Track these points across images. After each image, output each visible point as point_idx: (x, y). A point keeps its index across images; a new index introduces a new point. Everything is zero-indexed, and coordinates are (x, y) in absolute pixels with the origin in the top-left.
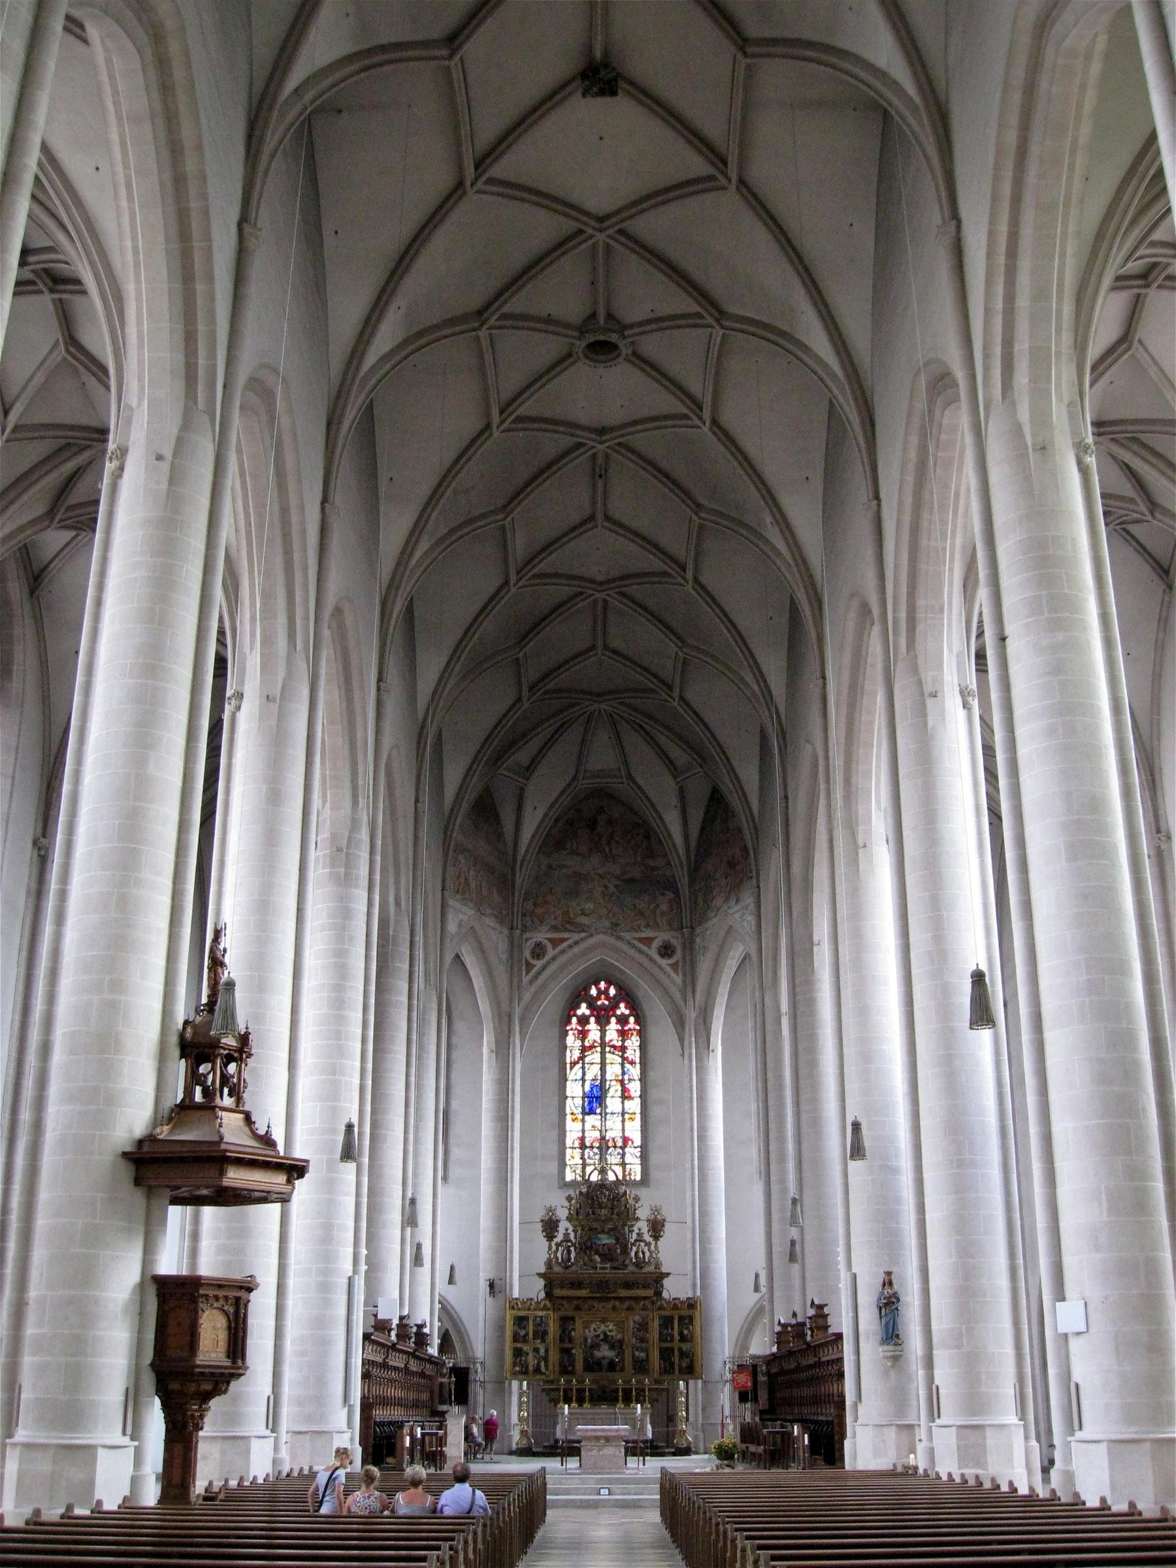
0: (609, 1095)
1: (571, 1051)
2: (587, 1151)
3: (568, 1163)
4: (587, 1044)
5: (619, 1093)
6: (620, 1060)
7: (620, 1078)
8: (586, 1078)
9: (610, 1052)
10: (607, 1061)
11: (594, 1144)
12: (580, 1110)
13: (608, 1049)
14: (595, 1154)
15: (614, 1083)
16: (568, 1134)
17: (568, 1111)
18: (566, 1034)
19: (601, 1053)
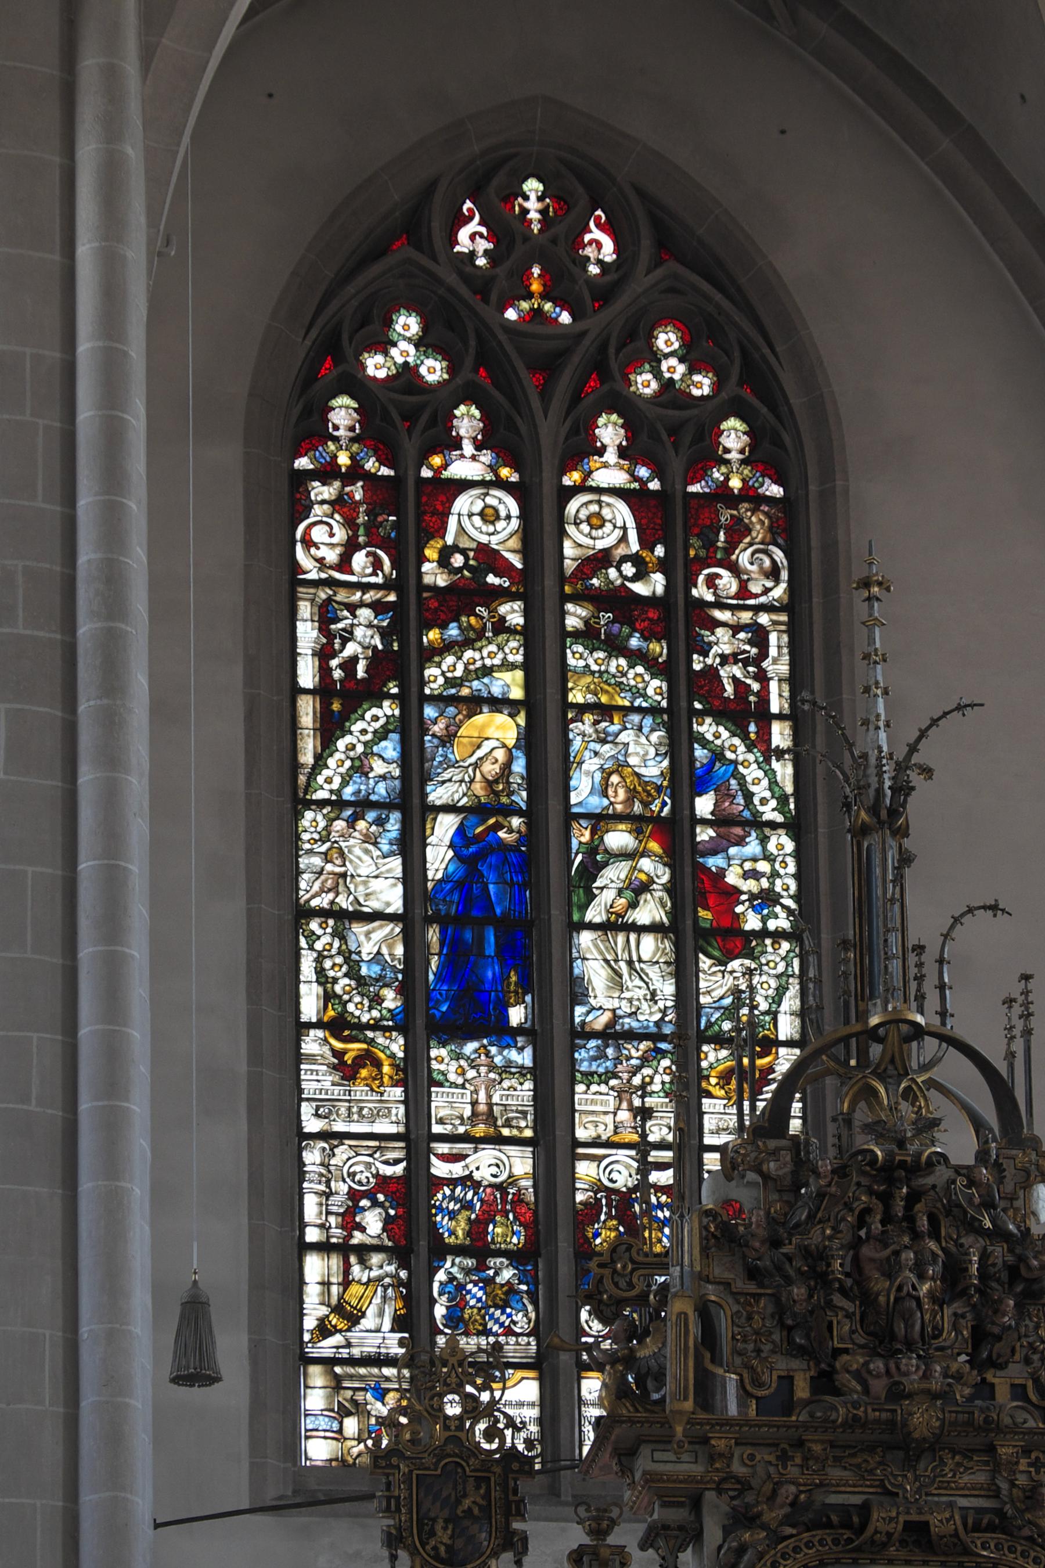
0: (595, 914)
1: (325, 617)
2: (451, 1267)
3: (313, 1352)
4: (433, 575)
5: (648, 912)
6: (655, 686)
7: (662, 806)
8: (438, 795)
9: (588, 635)
10: (577, 697)
11: (496, 1231)
12: (391, 1000)
13: (575, 617)
14: (504, 1300)
15: (618, 839)
16: (312, 1157)
17: (310, 1006)
18: (301, 508)
19: (529, 635)
